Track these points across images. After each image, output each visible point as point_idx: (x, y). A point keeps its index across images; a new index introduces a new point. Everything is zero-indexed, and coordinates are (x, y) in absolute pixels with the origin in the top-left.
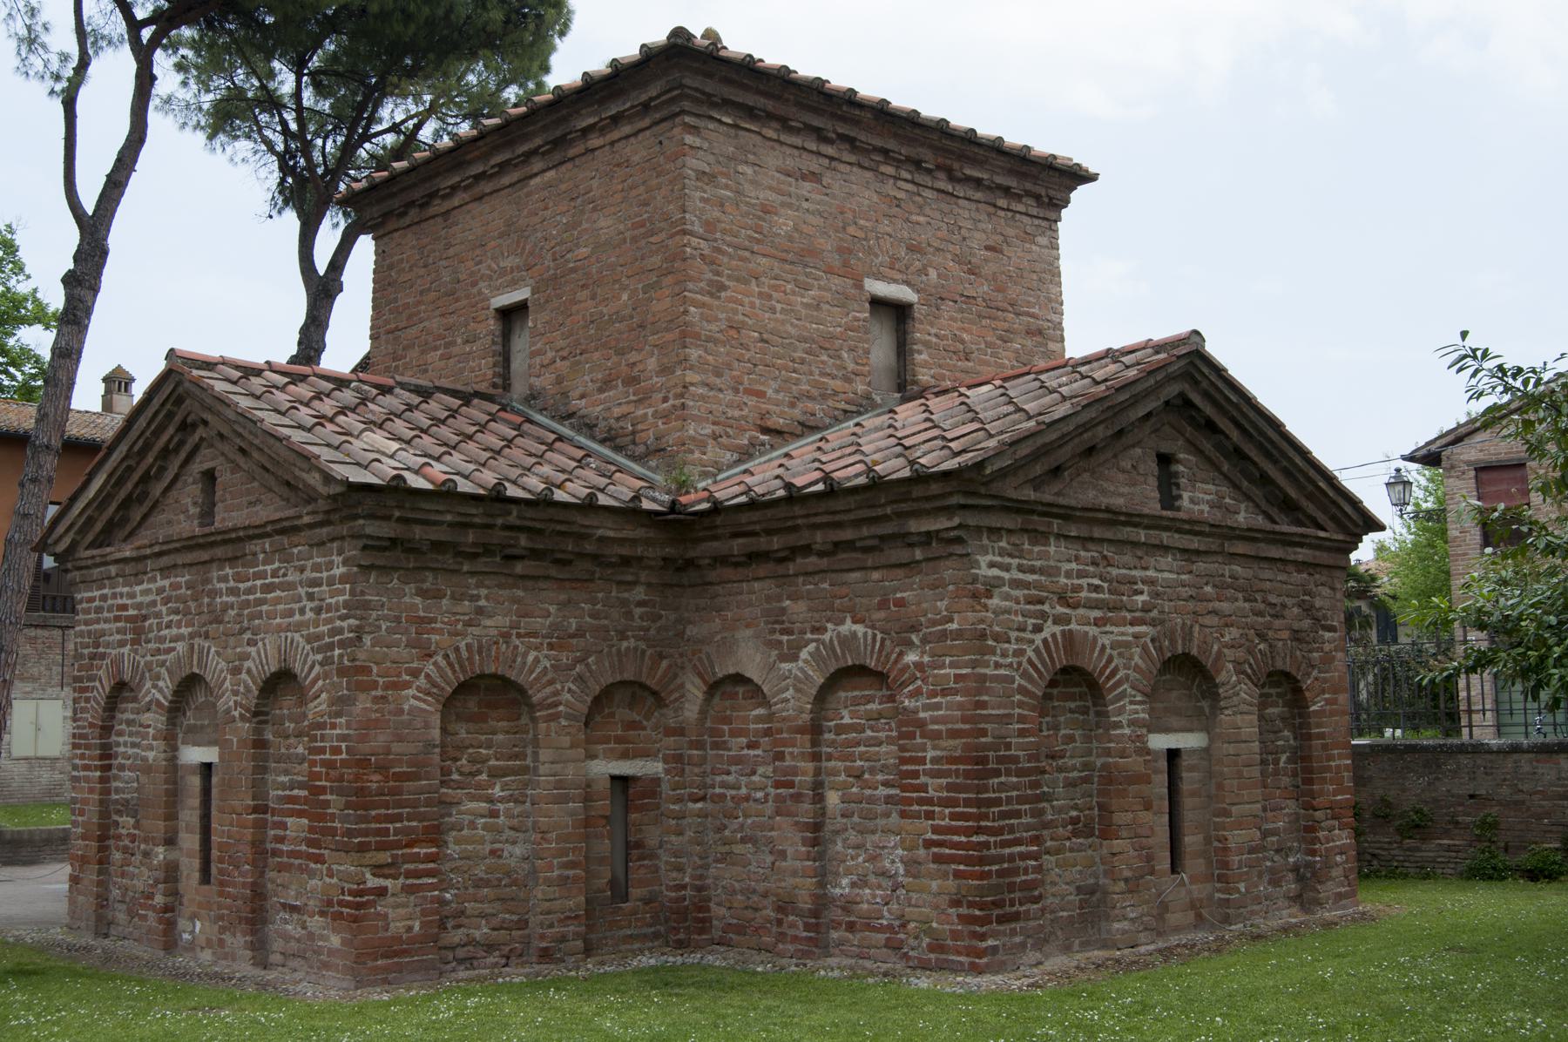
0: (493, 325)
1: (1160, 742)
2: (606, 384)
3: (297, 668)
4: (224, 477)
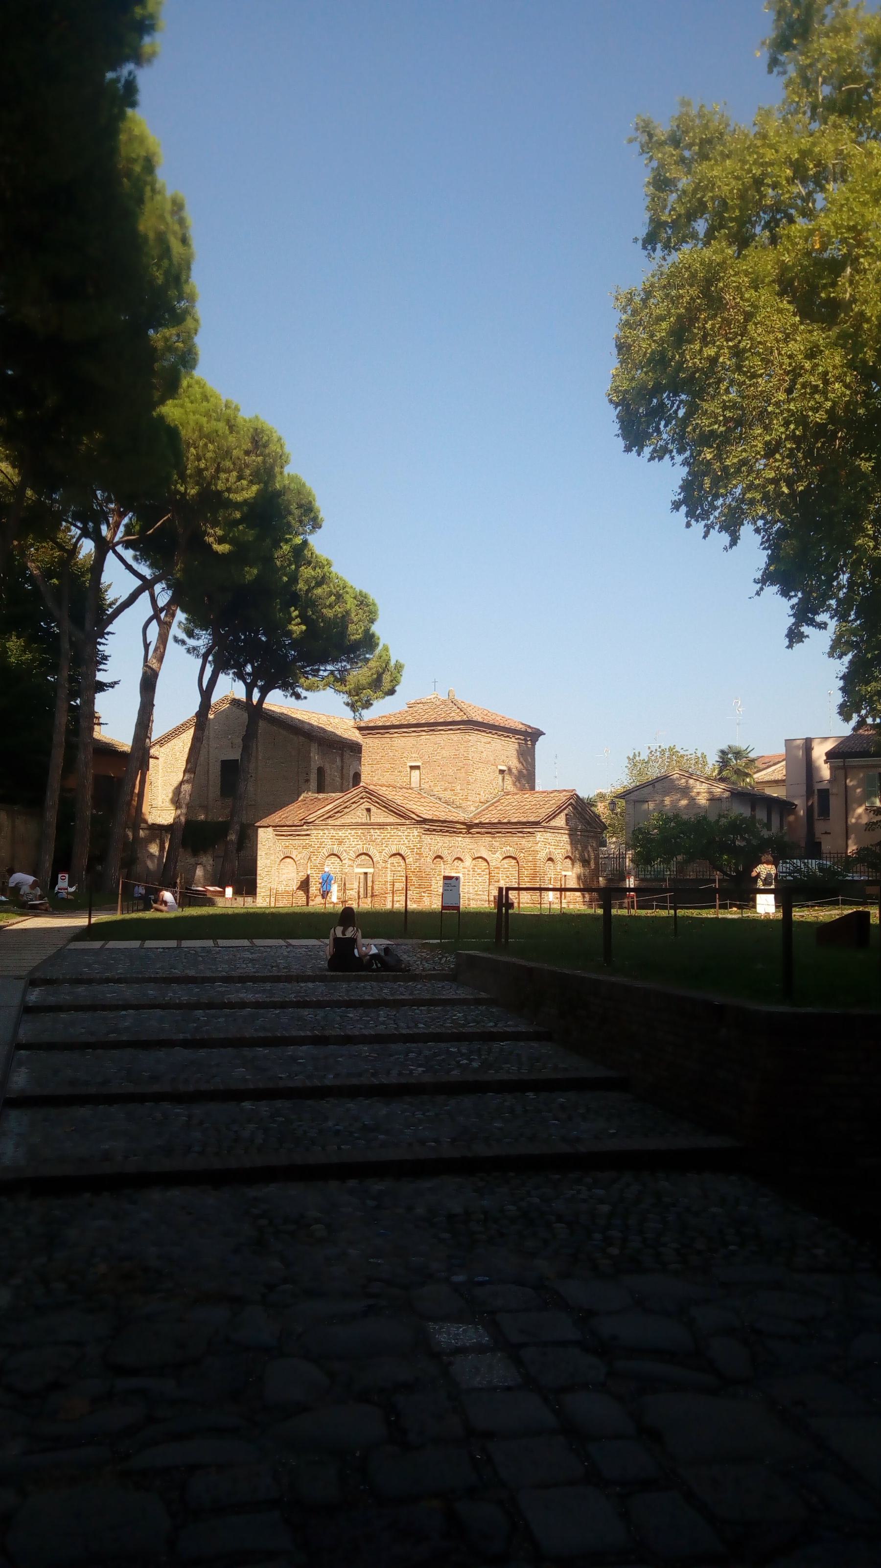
0: (409, 769)
1: (564, 873)
2: (445, 790)
3: (402, 853)
4: (373, 809)
